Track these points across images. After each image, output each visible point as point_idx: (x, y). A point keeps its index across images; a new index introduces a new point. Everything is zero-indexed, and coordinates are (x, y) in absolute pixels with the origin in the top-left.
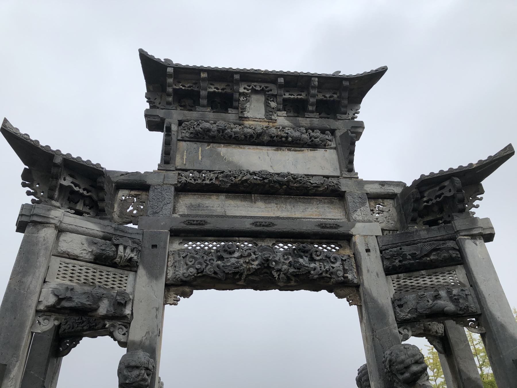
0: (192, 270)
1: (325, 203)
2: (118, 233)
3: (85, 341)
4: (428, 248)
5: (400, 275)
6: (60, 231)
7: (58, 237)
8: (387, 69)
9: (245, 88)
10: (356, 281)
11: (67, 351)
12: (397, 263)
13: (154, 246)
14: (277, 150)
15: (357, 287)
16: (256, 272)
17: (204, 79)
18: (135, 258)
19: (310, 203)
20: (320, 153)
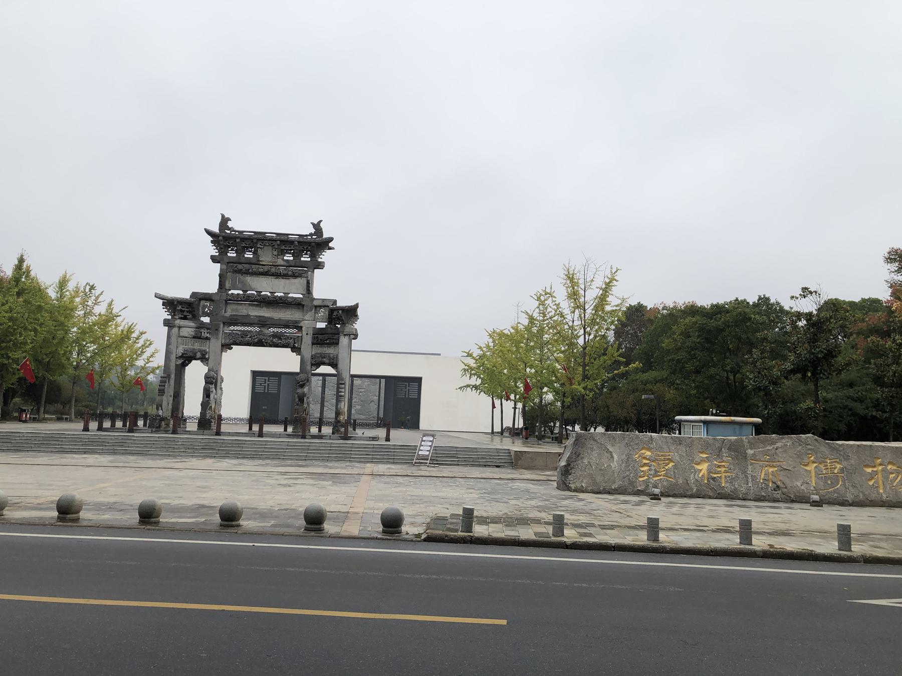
0: (231, 341)
1: (295, 309)
2: (202, 326)
3: (194, 362)
4: (326, 338)
5: (318, 345)
6: (180, 327)
7: (179, 330)
8: (332, 241)
9: (260, 245)
10: (299, 347)
11: (187, 365)
12: (315, 342)
13: (216, 330)
14: (276, 278)
15: (300, 348)
16: (256, 343)
17: (239, 242)
18: (209, 336)
19: (288, 308)
20: (298, 280)
